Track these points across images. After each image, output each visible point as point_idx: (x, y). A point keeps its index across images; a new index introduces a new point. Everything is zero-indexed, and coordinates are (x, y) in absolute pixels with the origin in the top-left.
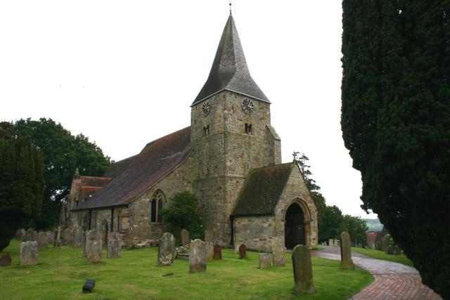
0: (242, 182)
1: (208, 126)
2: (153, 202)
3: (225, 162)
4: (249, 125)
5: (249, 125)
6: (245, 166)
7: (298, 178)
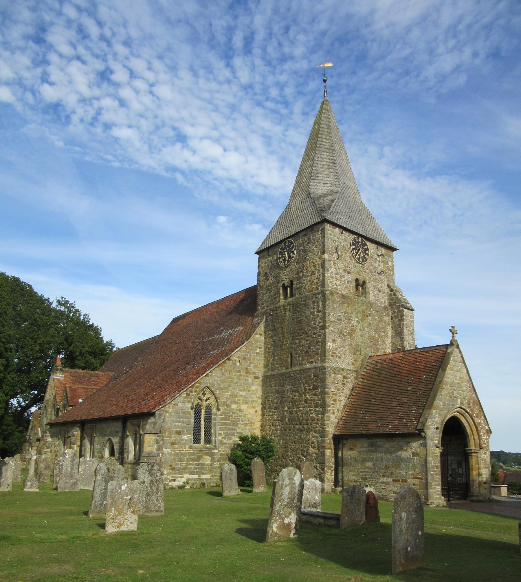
0: (352, 379)
1: (292, 283)
2: (197, 410)
3: (324, 342)
4: (361, 282)
5: (361, 282)
6: (356, 350)
7: (460, 371)
